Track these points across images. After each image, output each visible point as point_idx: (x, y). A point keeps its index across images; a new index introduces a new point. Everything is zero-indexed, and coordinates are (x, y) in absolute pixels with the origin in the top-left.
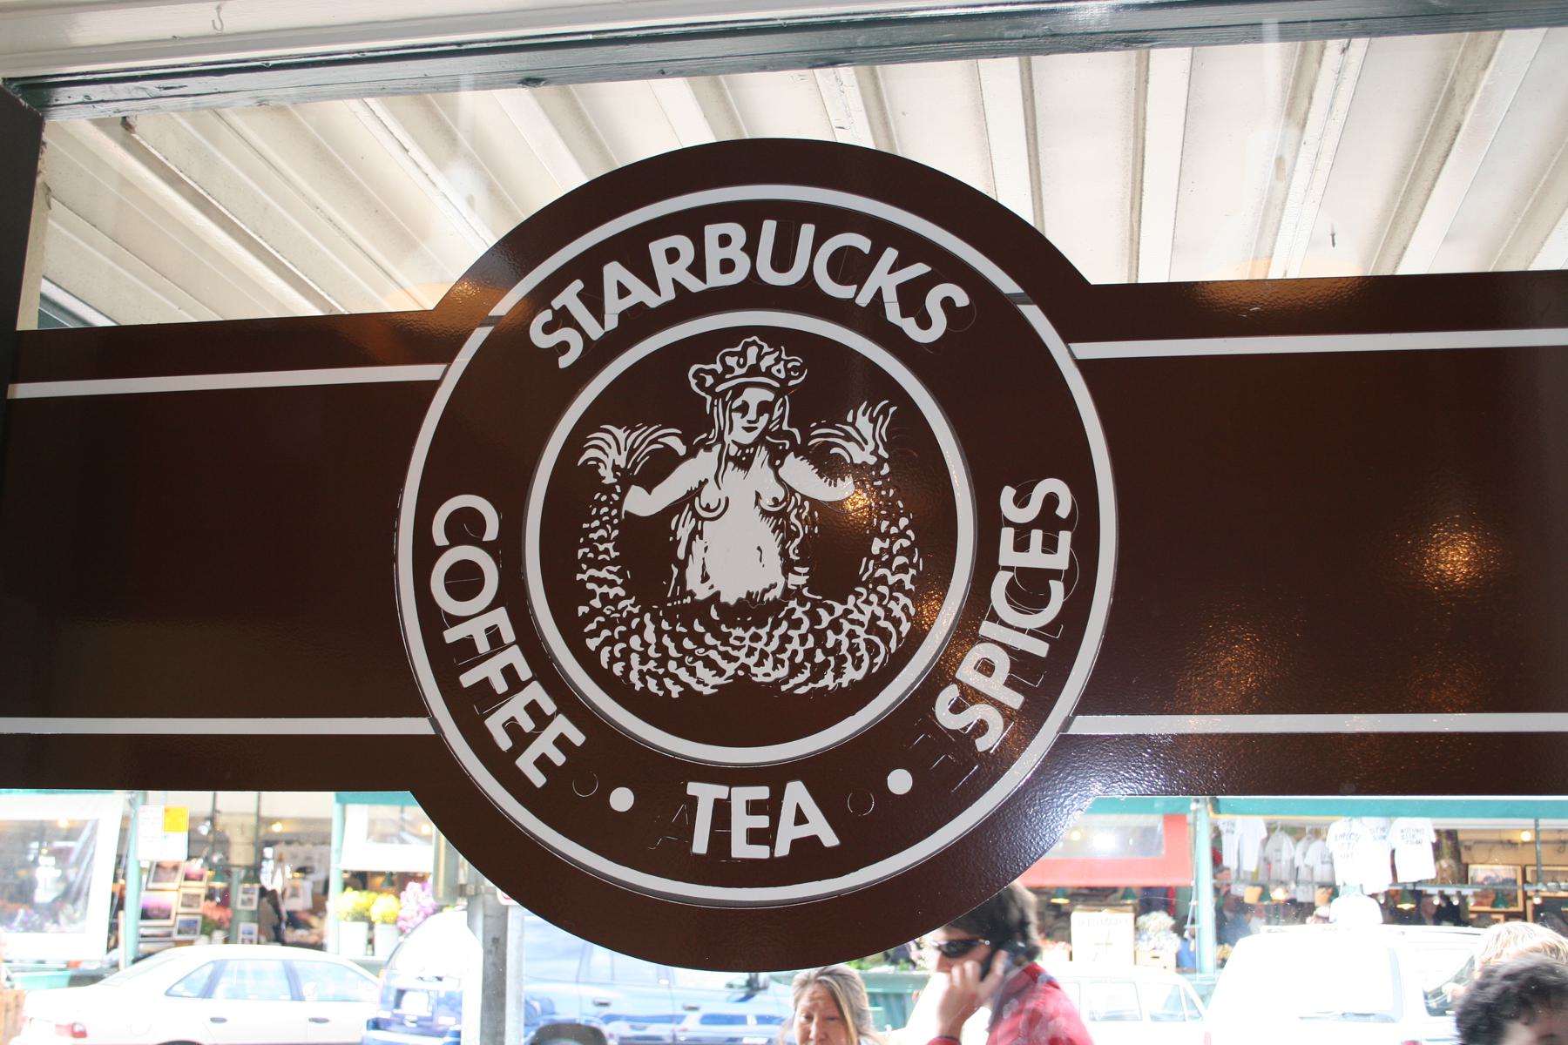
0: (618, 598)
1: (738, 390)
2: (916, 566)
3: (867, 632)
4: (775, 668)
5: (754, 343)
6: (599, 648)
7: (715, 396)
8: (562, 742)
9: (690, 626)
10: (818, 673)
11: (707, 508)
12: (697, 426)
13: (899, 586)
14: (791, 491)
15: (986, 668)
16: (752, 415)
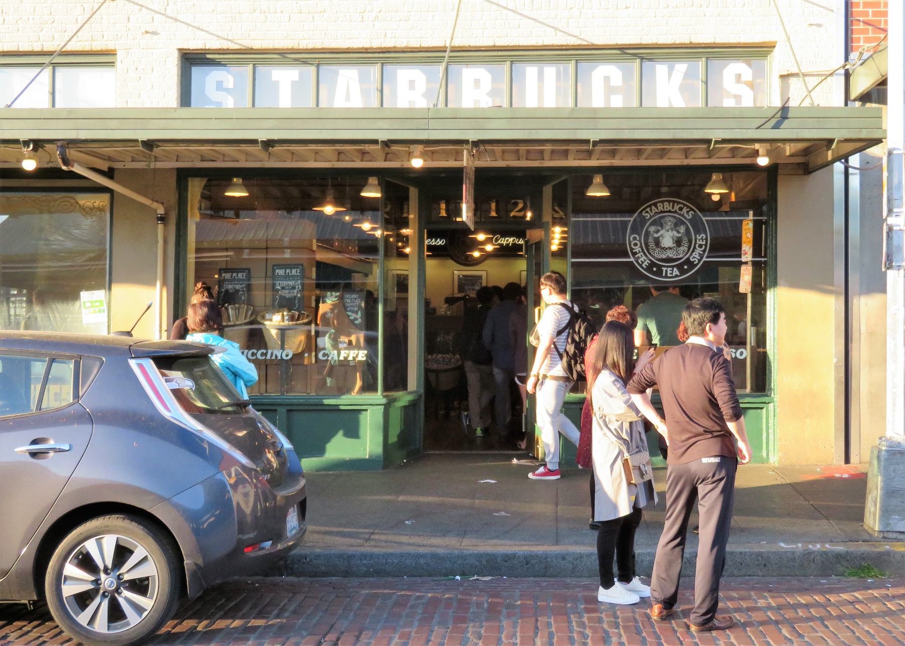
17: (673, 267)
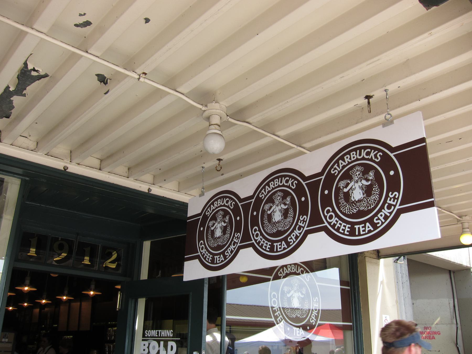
10: (368, 207)
12: (351, 178)
17: (364, 222)
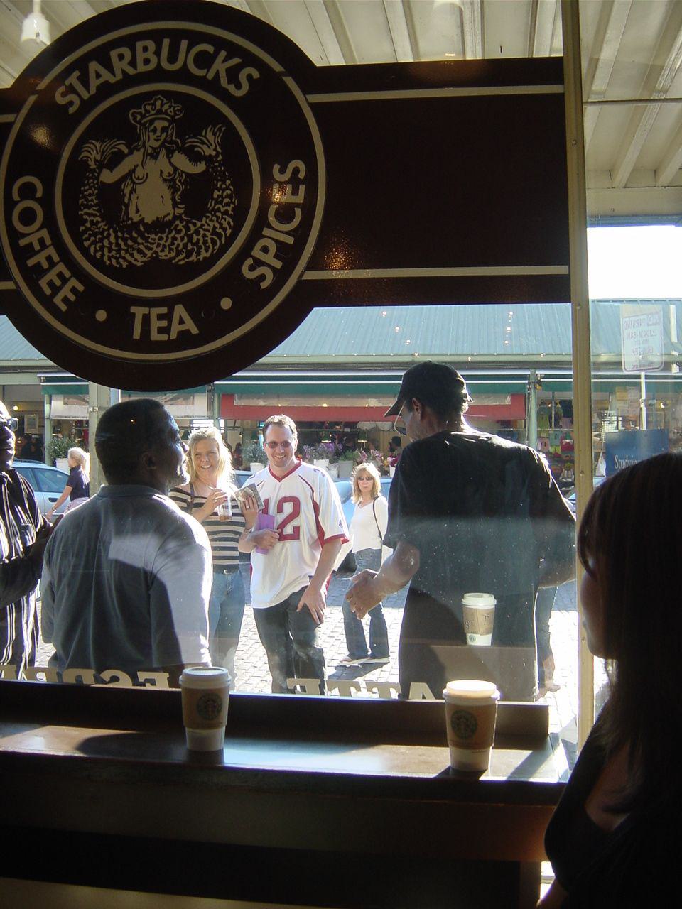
0: (98, 222)
1: (152, 122)
2: (234, 203)
3: (211, 235)
4: (169, 252)
5: (159, 99)
6: (90, 246)
7: (142, 125)
8: (74, 290)
9: (130, 234)
11: (138, 179)
12: (133, 140)
13: (226, 213)
14: (176, 169)
15: (265, 250)
16: (158, 133)
